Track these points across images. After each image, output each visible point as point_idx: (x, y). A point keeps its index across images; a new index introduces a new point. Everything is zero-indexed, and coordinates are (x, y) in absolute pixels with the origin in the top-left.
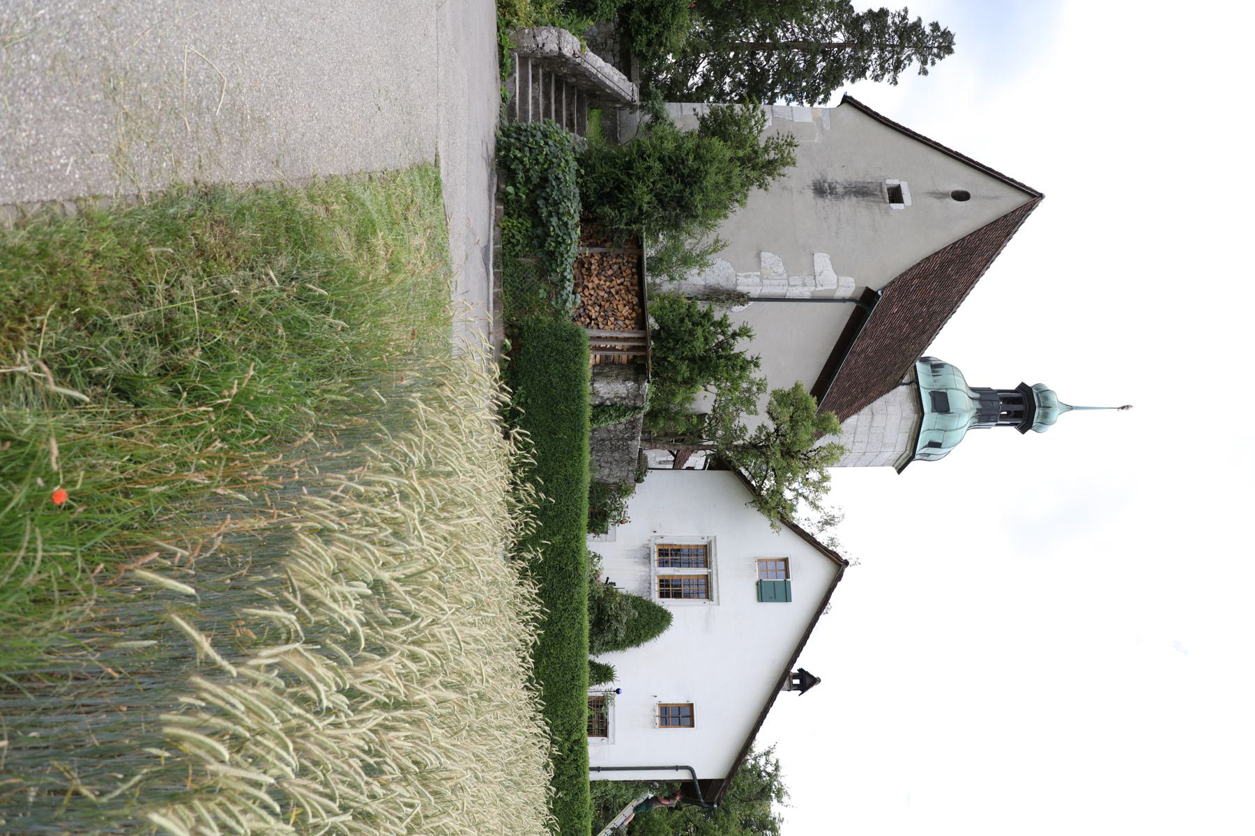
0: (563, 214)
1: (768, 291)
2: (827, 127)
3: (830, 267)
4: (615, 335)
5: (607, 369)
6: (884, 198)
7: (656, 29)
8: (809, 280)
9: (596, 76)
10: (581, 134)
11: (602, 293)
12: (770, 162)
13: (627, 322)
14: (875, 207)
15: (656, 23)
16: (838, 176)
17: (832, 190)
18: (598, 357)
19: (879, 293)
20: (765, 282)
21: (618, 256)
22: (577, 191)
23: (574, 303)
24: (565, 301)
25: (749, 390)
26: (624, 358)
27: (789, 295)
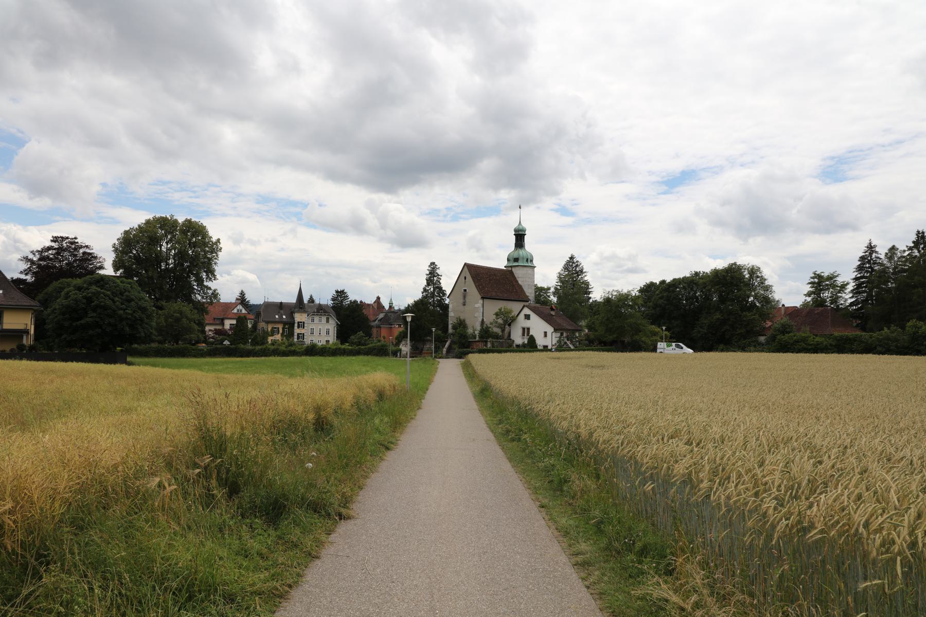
16: (462, 301)
17: (464, 302)
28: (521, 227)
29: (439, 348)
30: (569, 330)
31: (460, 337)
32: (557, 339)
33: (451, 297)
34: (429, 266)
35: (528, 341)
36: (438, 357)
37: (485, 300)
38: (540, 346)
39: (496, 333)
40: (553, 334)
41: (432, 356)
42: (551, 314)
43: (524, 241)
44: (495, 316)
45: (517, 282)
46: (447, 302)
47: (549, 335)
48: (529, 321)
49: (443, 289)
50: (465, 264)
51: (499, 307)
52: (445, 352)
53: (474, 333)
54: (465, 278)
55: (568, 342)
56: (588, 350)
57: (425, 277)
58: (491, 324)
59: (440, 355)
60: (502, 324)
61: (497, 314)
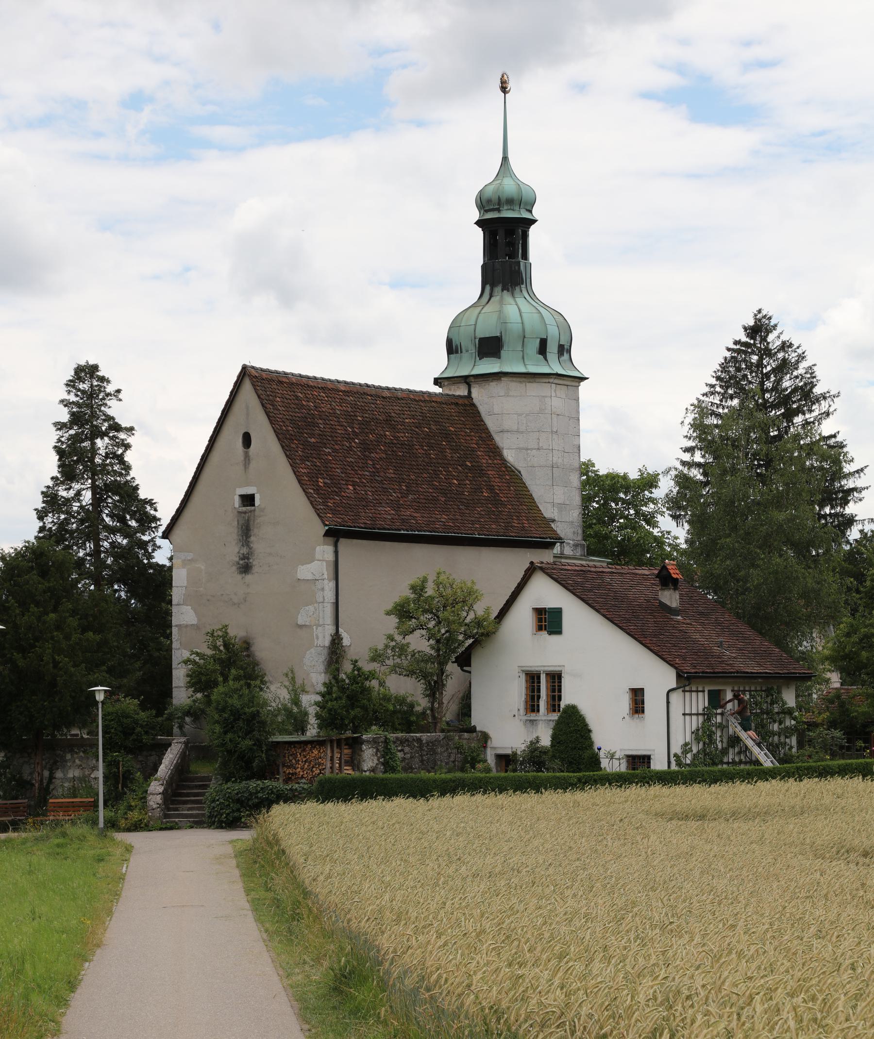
0: (257, 790)
1: (329, 618)
2: (190, 556)
3: (308, 566)
4: (329, 758)
5: (356, 762)
6: (251, 511)
7: (139, 729)
8: (319, 585)
9: (172, 770)
10: (210, 780)
11: (306, 766)
12: (226, 645)
13: (321, 751)
14: (258, 520)
15: (134, 729)
16: (233, 551)
17: (245, 557)
18: (345, 768)
19: (327, 528)
20: (321, 622)
21: (285, 757)
22: (244, 782)
23: (304, 783)
24: (303, 788)
25: (393, 649)
26: (347, 751)
27: (333, 600)
28: (508, 187)
29: (127, 777)
30: (750, 677)
31: (228, 727)
32: (695, 722)
33: (177, 533)
34: (71, 384)
35: (554, 737)
36: (123, 823)
37: (343, 543)
38: (612, 756)
39: (401, 701)
40: (677, 699)
41: (95, 822)
42: (664, 607)
43: (525, 256)
44: (394, 620)
45: (495, 452)
46: (161, 557)
47: (654, 702)
48: (555, 638)
49: (143, 494)
50: (245, 372)
51: (413, 579)
52: (159, 799)
53: (296, 702)
54: (247, 440)
55: (748, 738)
56: (843, 772)
57: (52, 436)
58: (377, 657)
59: (135, 815)
60: (427, 659)
61: (402, 612)
